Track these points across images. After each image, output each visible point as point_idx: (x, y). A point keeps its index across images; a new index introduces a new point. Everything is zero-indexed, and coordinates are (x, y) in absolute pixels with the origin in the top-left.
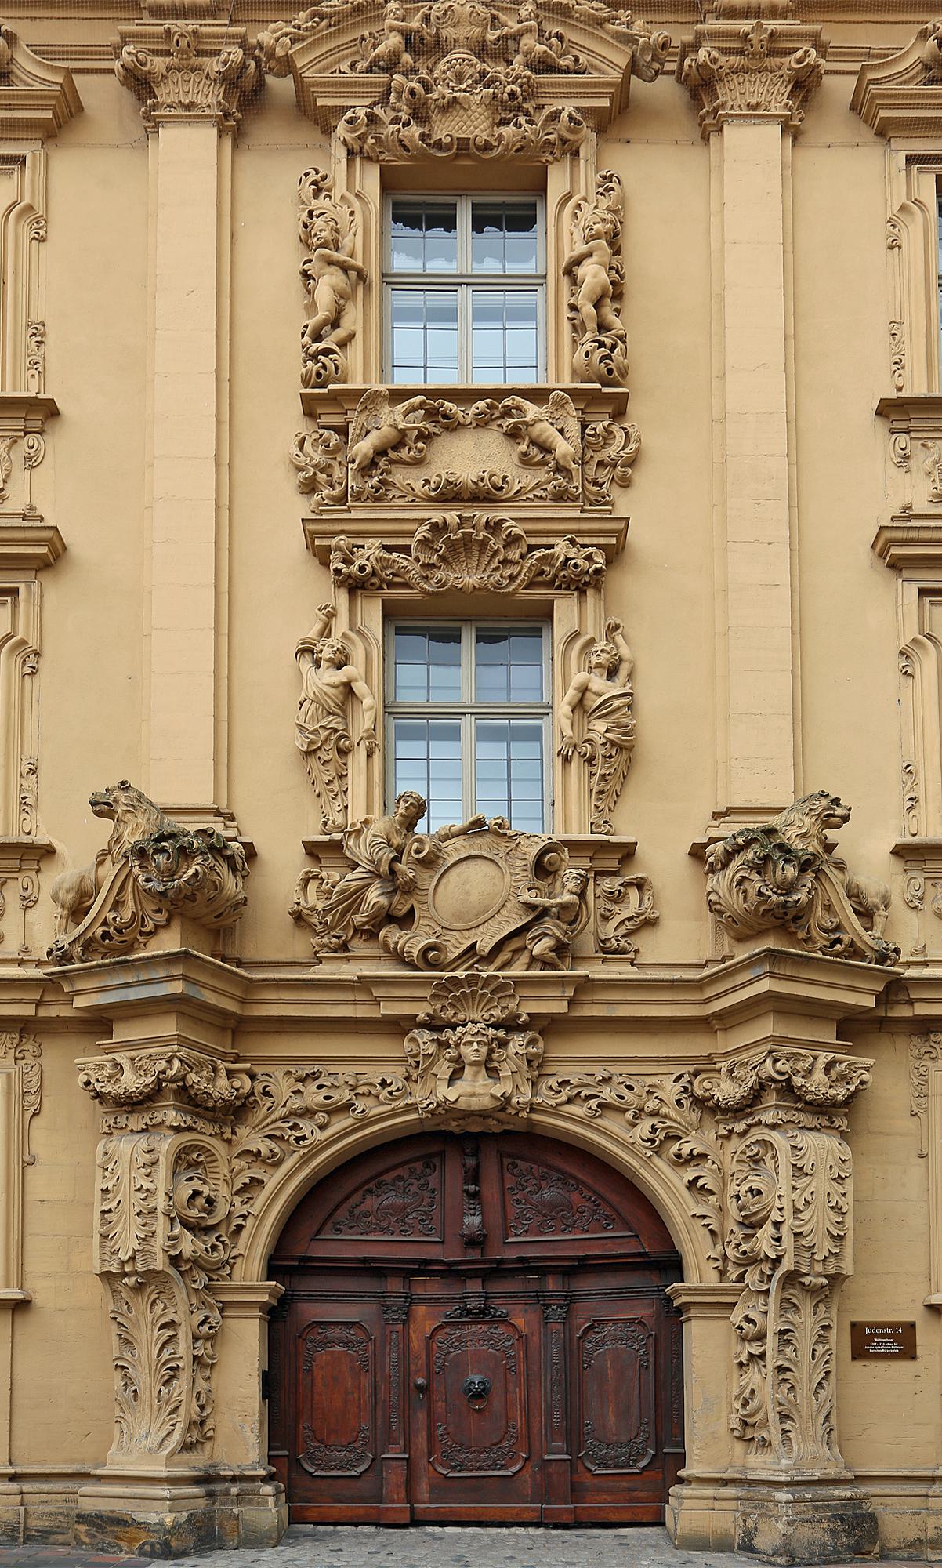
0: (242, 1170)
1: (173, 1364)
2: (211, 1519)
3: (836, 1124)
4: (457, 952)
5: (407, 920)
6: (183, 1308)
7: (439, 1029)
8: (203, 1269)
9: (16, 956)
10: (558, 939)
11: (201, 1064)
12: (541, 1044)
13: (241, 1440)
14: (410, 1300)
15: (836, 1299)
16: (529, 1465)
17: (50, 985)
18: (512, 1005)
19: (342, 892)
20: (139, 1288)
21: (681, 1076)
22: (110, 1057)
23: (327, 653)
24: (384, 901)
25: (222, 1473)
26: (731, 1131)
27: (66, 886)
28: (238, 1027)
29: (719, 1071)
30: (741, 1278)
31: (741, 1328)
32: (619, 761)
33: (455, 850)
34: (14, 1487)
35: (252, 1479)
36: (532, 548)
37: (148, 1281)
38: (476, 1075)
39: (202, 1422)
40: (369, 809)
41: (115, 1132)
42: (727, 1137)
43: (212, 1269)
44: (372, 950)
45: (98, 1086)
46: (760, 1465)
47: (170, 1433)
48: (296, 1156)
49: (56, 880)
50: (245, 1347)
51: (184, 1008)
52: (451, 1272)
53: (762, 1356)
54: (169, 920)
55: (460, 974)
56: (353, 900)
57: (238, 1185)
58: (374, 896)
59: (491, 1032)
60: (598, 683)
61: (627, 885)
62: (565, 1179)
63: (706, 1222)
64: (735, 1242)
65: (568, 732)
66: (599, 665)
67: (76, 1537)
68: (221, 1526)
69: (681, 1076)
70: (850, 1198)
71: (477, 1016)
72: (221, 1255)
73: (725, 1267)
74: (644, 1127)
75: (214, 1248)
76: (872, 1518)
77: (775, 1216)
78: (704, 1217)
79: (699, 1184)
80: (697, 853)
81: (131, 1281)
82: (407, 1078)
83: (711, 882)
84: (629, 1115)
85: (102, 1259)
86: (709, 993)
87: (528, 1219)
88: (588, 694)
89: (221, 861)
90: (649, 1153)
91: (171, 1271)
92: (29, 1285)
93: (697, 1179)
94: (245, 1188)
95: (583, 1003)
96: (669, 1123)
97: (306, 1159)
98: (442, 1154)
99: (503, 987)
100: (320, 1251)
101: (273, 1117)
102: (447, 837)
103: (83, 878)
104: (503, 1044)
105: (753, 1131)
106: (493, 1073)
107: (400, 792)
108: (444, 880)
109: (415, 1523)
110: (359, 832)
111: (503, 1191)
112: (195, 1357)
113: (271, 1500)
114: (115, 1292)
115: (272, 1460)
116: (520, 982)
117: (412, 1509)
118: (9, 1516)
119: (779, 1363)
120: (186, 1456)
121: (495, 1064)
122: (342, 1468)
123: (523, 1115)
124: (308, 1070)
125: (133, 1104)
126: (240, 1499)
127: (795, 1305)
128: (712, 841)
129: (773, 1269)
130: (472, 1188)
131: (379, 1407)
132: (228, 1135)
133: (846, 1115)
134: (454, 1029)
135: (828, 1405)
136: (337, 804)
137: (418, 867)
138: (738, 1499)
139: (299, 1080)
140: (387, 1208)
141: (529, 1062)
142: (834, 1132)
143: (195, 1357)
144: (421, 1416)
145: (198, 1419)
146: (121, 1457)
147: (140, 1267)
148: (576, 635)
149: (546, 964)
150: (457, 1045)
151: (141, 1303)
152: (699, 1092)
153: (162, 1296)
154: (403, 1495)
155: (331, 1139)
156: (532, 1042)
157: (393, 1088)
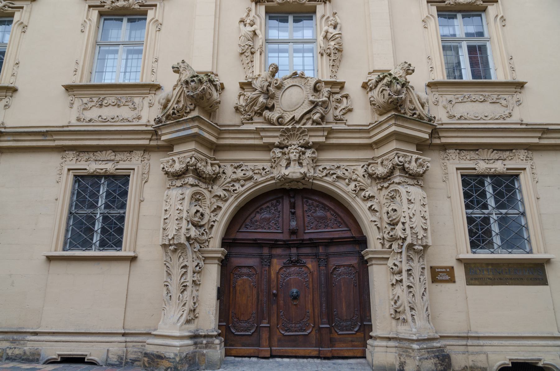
0: (214, 203)
1: (185, 284)
2: (195, 356)
3: (420, 183)
4: (288, 120)
5: (272, 109)
6: (190, 259)
7: (282, 148)
8: (198, 243)
9: (145, 123)
10: (322, 114)
11: (202, 160)
12: (316, 153)
13: (209, 320)
14: (271, 256)
15: (426, 256)
16: (314, 330)
17: (155, 133)
18: (307, 138)
19: (251, 98)
20: (175, 251)
21: (364, 166)
22: (171, 158)
23: (248, 21)
25: (201, 334)
27: (163, 97)
28: (216, 148)
29: (377, 163)
30: (390, 247)
31: (392, 269)
32: (338, 55)
33: (288, 83)
34: (123, 339)
35: (211, 336)
37: (178, 248)
38: (295, 165)
39: (194, 310)
40: (260, 71)
41: (172, 187)
42: (381, 189)
43: (201, 243)
44: (261, 119)
45: (166, 169)
46: (404, 331)
47: (182, 315)
49: (161, 96)
50: (212, 276)
52: (286, 245)
53: (401, 281)
54: (195, 108)
56: (254, 101)
57: (213, 209)
58: (262, 99)
59: (300, 148)
60: (331, 30)
62: (325, 207)
63: (376, 223)
64: (387, 232)
65: (322, 45)
66: (331, 25)
67: (144, 363)
68: (198, 358)
69: (364, 166)
71: (295, 143)
72: (205, 237)
73: (384, 242)
75: (203, 234)
76: (448, 357)
78: (375, 221)
79: (373, 208)
80: (365, 86)
81: (172, 248)
82: (271, 167)
83: (370, 94)
84: (347, 181)
85: (163, 239)
86: (372, 134)
87: (312, 223)
88: (328, 34)
90: (355, 195)
91: (186, 243)
92: (137, 250)
93: (372, 206)
94: (215, 210)
95: (330, 138)
96: (361, 184)
97: (236, 198)
98: (282, 198)
99: (304, 132)
100: (240, 236)
101: (226, 182)
102: (285, 79)
103: (168, 95)
104: (304, 153)
105: (391, 186)
106: (300, 164)
107: (270, 64)
108: (284, 94)
109: (272, 356)
110: (257, 78)
111: (303, 211)
112: (194, 281)
113: (218, 346)
114: (166, 252)
115: (220, 327)
117: (271, 349)
118: (120, 353)
119: (408, 284)
120: (187, 326)
121: (301, 161)
123: (311, 180)
124: (238, 164)
125: (178, 175)
126: (207, 346)
127: (412, 258)
128: (370, 80)
130: (293, 211)
131: (260, 303)
132: (210, 189)
134: (287, 148)
135: (427, 303)
136: (251, 70)
138: (396, 347)
139: (236, 168)
140: (263, 219)
141: (313, 160)
142: (419, 187)
143: (194, 281)
144: (275, 307)
145: (193, 309)
147: (176, 242)
148: (324, 16)
149: (318, 123)
150: (289, 154)
151: (175, 257)
153: (183, 254)
155: (245, 191)
156: (313, 153)
157: (267, 170)
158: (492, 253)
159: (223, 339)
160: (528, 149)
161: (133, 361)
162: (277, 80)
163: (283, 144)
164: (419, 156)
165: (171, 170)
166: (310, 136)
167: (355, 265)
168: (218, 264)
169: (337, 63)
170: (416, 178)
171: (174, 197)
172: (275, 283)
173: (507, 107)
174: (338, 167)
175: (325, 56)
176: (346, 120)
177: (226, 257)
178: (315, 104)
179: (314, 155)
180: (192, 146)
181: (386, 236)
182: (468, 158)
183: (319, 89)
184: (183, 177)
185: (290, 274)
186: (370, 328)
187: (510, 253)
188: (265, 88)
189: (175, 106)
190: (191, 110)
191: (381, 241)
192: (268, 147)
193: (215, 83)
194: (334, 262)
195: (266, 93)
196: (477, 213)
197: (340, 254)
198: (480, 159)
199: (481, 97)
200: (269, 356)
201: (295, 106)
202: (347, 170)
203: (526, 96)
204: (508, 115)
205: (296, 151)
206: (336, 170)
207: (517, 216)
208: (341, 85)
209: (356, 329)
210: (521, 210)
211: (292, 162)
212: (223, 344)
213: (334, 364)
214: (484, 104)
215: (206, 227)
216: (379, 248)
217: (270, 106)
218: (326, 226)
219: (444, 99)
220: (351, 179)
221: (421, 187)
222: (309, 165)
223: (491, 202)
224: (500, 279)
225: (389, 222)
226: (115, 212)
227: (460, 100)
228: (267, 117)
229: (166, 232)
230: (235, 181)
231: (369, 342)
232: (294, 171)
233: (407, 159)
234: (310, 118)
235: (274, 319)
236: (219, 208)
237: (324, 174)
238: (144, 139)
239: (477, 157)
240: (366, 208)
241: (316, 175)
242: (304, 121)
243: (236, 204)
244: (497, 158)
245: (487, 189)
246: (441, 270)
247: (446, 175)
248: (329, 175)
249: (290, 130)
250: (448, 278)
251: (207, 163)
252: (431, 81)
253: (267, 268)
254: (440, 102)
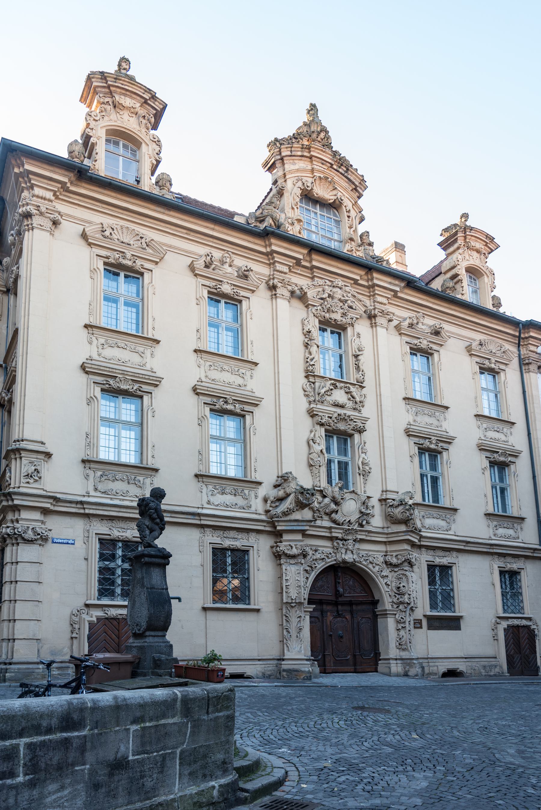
30: (397, 607)
36: (354, 422)
71: (350, 538)
86: (389, 536)
106: (352, 552)
146: (289, 653)
216: (390, 608)
232: (349, 557)
238: (261, 525)
240: (384, 583)
250: (419, 626)
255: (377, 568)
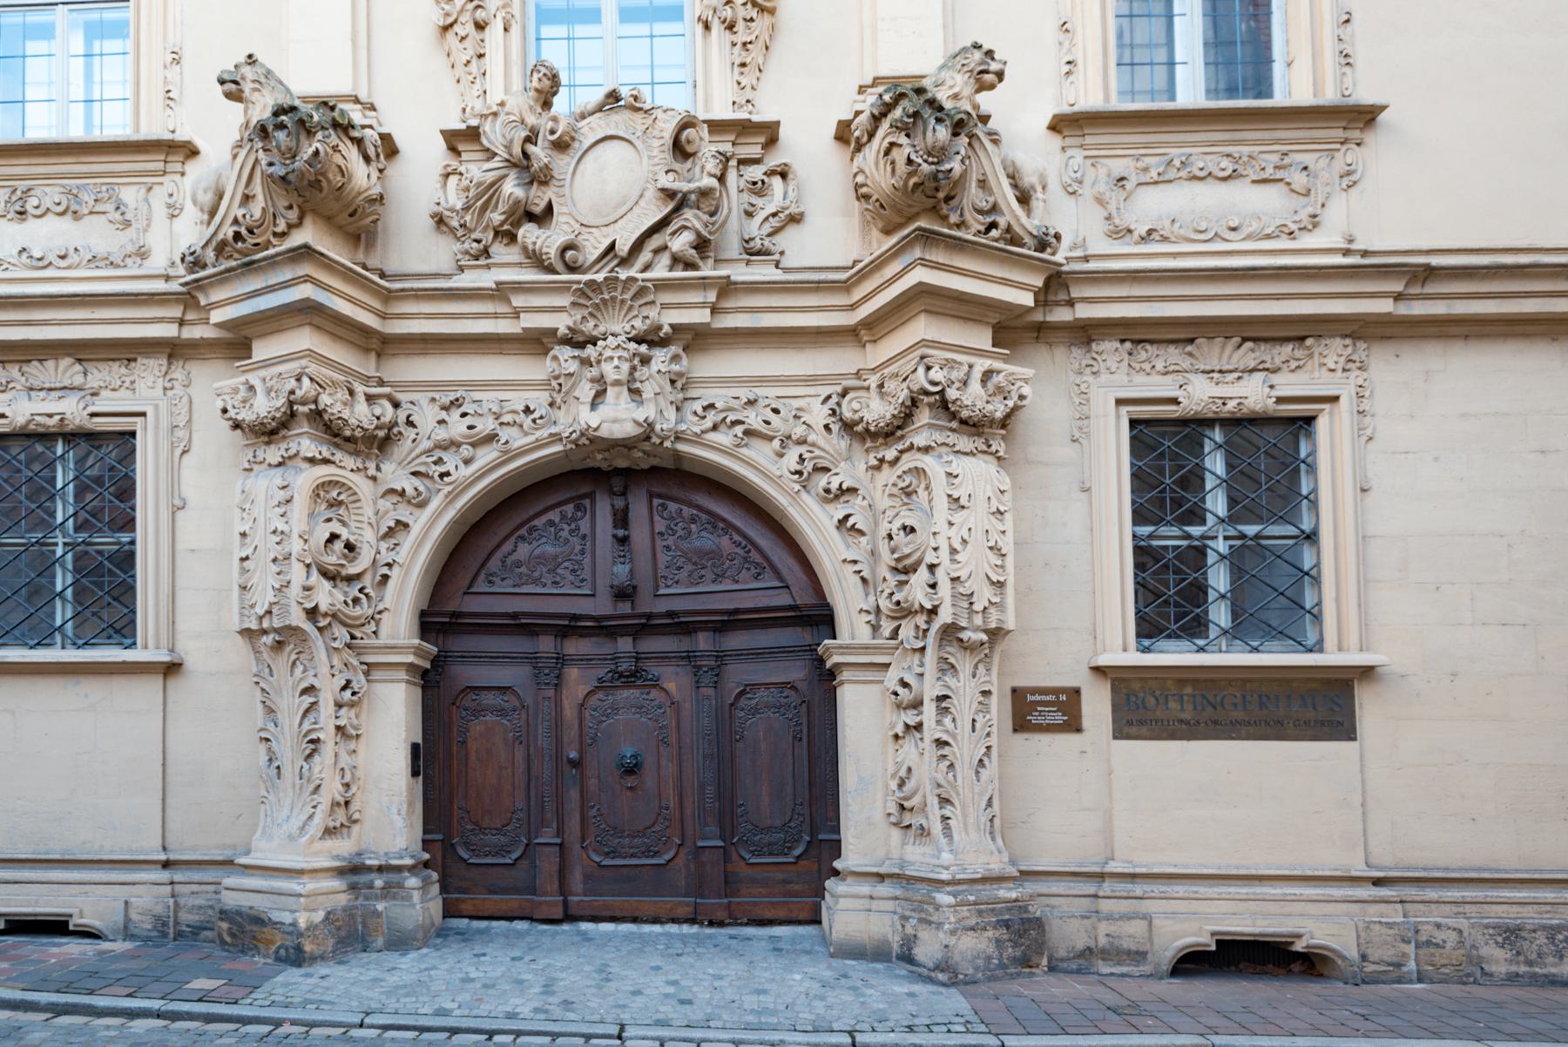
0: (387, 512)
3: (993, 449)
4: (597, 253)
5: (544, 217)
7: (581, 345)
10: (698, 234)
11: (334, 383)
12: (685, 361)
16: (683, 851)
18: (653, 313)
19: (479, 185)
21: (829, 397)
22: (242, 379)
24: (519, 193)
26: (882, 460)
29: (868, 389)
38: (617, 397)
42: (878, 468)
45: (232, 413)
48: (441, 495)
50: (394, 715)
51: (317, 320)
52: (603, 628)
55: (600, 277)
57: (384, 530)
59: (633, 346)
61: (771, 173)
63: (857, 568)
64: (888, 591)
69: (829, 397)
70: (1010, 534)
71: (617, 328)
72: (364, 610)
74: (793, 454)
75: (356, 601)
77: (930, 558)
78: (855, 562)
79: (849, 524)
80: (843, 134)
82: (551, 405)
84: (776, 443)
86: (858, 294)
89: (349, 143)
90: (797, 487)
93: (847, 517)
94: (390, 532)
95: (726, 311)
97: (452, 497)
99: (642, 291)
104: (646, 361)
105: (905, 456)
106: (635, 393)
108: (581, 167)
109: (570, 917)
115: (426, 845)
116: (662, 285)
117: (565, 903)
121: (638, 385)
122: (496, 854)
123: (667, 444)
124: (452, 396)
128: (858, 113)
129: (927, 622)
130: (621, 533)
133: (1004, 438)
134: (595, 344)
137: (554, 153)
141: (673, 382)
144: (574, 794)
149: (690, 265)
150: (599, 362)
152: (848, 415)
154: (556, 886)
155: (475, 475)
157: (536, 415)
158: (1201, 650)
159: (435, 876)
160: (1355, 336)
161: (196, 930)
162: (555, 119)
163: (582, 332)
164: (997, 365)
165: (246, 416)
166: (665, 306)
167: (797, 685)
168: (408, 682)
169: (756, 53)
170: (987, 429)
171: (262, 497)
172: (574, 732)
173: (1307, 193)
174: (751, 403)
175: (716, 27)
176: (782, 253)
177: (436, 661)
178: (678, 202)
179: (675, 368)
180: (303, 339)
181: (885, 604)
182: (1160, 366)
183: (690, 149)
184: (284, 437)
185: (616, 709)
186: (836, 849)
187: (1256, 650)
188: (517, 150)
189: (240, 213)
190: (290, 226)
191: (872, 617)
192: (537, 343)
193: (355, 134)
194: (738, 674)
195: (522, 164)
196: (1169, 537)
197: (757, 654)
198: (1196, 371)
199: (1225, 163)
200: (560, 916)
201: (617, 207)
202: (776, 411)
203: (1376, 156)
204: (1307, 223)
205: (620, 353)
206: (746, 413)
207: (1291, 542)
208: (770, 133)
209: (797, 852)
210: (1307, 526)
211: (609, 389)
212: (436, 888)
213: (732, 937)
214: (1231, 184)
215: (367, 581)
216: (864, 635)
217: (537, 210)
218: (719, 578)
219: (1102, 172)
220: (789, 437)
221: (999, 458)
222: (660, 398)
223: (1217, 503)
224: (1215, 722)
225: (893, 564)
226: (106, 541)
227: (1154, 174)
228: (530, 247)
229: (248, 596)
230: (445, 448)
231: (829, 884)
232: (617, 418)
233: (955, 375)
234: (665, 248)
235: (574, 824)
236: (402, 525)
237: (708, 423)
239: (1186, 363)
240: (830, 526)
241: (683, 427)
242: (645, 256)
243: (450, 514)
244: (1252, 364)
245: (1208, 463)
246: (1044, 698)
247: (1082, 420)
248: (723, 428)
249: (601, 281)
250: (1059, 718)
251: (351, 393)
252: (1066, 109)
253: (551, 693)
254: (1088, 181)
255: (793, 454)
